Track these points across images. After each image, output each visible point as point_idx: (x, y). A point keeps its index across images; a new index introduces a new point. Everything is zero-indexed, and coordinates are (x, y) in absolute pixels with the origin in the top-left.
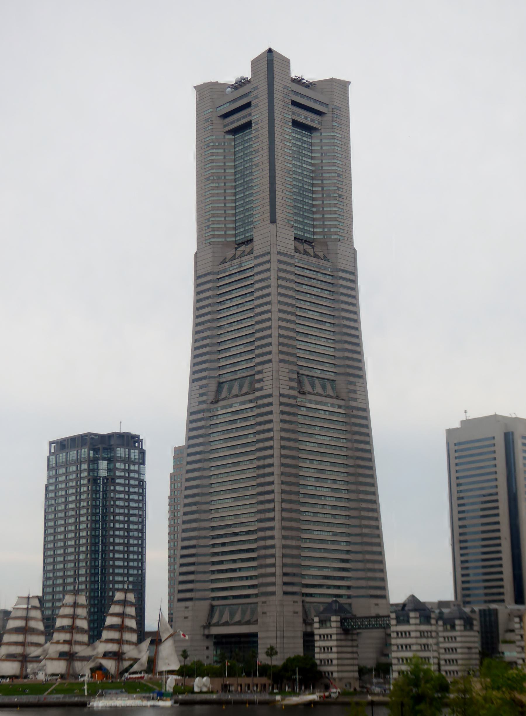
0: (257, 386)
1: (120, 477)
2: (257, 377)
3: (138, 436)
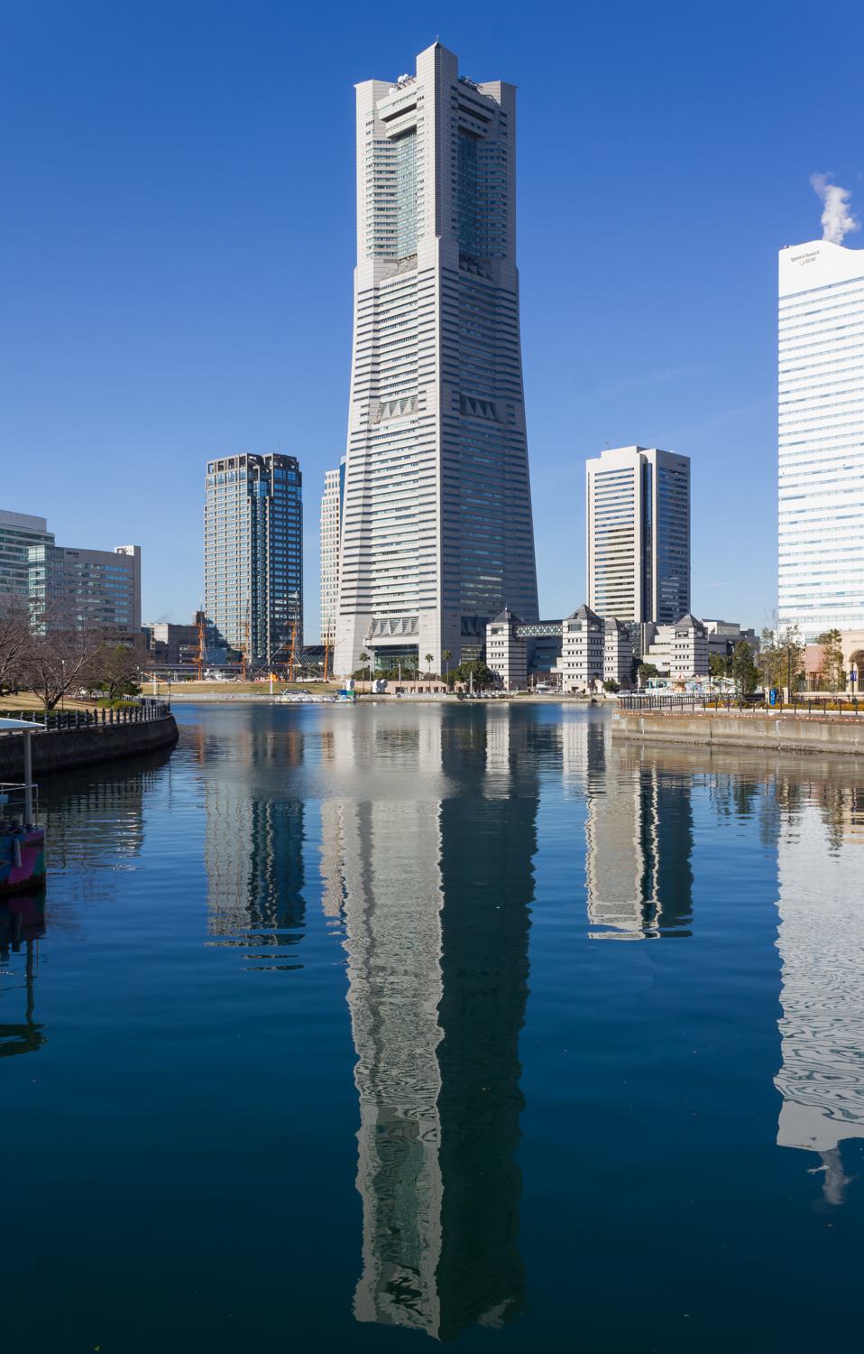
0: (421, 405)
2: (421, 397)
3: (295, 459)
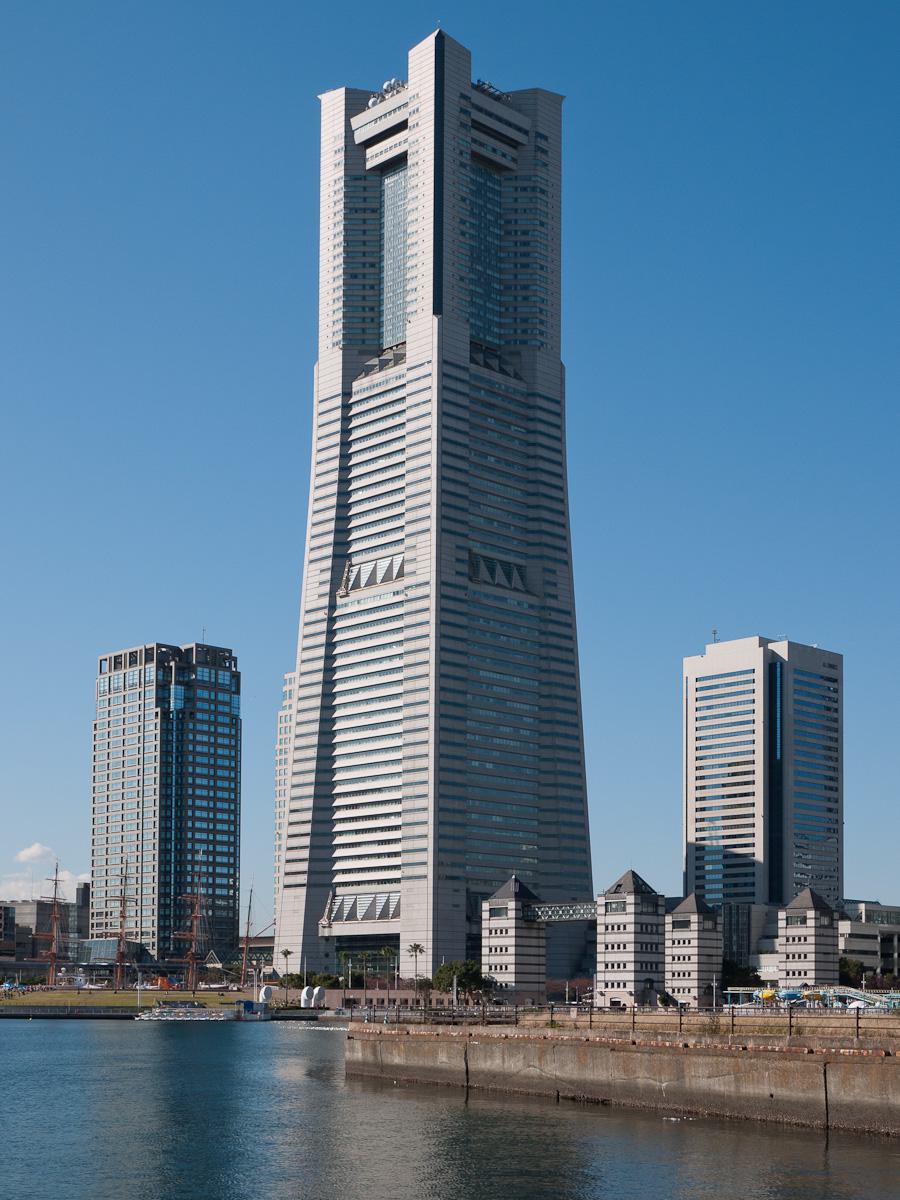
1: (202, 711)
